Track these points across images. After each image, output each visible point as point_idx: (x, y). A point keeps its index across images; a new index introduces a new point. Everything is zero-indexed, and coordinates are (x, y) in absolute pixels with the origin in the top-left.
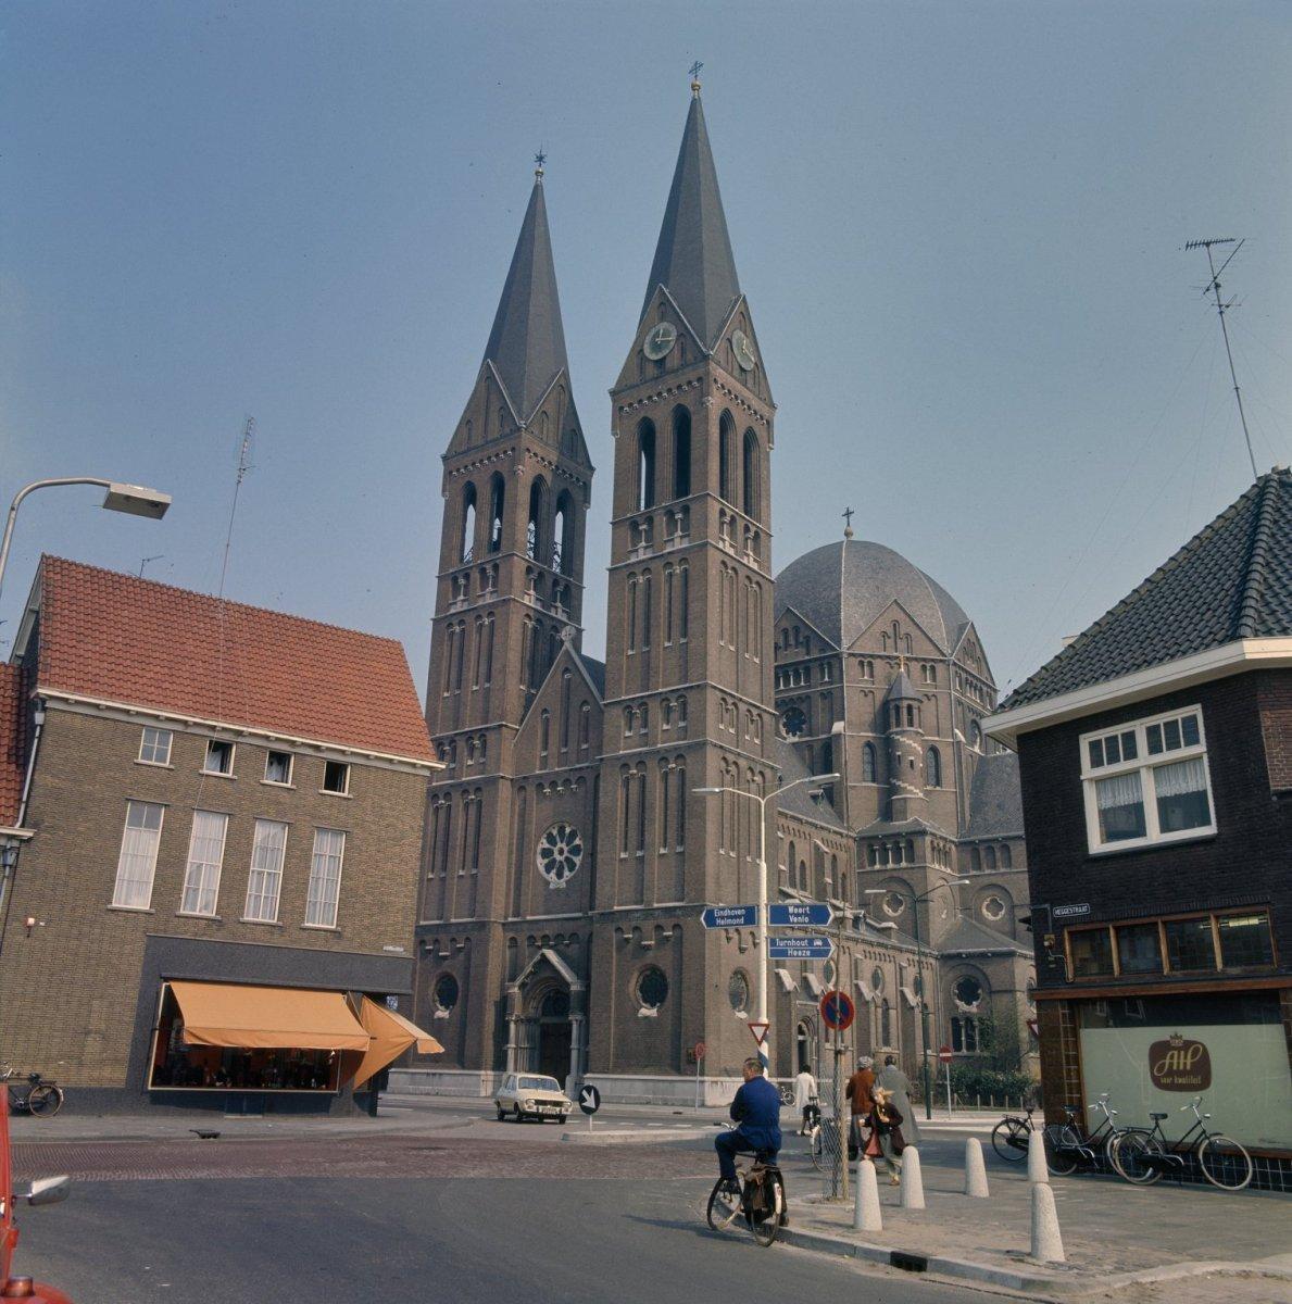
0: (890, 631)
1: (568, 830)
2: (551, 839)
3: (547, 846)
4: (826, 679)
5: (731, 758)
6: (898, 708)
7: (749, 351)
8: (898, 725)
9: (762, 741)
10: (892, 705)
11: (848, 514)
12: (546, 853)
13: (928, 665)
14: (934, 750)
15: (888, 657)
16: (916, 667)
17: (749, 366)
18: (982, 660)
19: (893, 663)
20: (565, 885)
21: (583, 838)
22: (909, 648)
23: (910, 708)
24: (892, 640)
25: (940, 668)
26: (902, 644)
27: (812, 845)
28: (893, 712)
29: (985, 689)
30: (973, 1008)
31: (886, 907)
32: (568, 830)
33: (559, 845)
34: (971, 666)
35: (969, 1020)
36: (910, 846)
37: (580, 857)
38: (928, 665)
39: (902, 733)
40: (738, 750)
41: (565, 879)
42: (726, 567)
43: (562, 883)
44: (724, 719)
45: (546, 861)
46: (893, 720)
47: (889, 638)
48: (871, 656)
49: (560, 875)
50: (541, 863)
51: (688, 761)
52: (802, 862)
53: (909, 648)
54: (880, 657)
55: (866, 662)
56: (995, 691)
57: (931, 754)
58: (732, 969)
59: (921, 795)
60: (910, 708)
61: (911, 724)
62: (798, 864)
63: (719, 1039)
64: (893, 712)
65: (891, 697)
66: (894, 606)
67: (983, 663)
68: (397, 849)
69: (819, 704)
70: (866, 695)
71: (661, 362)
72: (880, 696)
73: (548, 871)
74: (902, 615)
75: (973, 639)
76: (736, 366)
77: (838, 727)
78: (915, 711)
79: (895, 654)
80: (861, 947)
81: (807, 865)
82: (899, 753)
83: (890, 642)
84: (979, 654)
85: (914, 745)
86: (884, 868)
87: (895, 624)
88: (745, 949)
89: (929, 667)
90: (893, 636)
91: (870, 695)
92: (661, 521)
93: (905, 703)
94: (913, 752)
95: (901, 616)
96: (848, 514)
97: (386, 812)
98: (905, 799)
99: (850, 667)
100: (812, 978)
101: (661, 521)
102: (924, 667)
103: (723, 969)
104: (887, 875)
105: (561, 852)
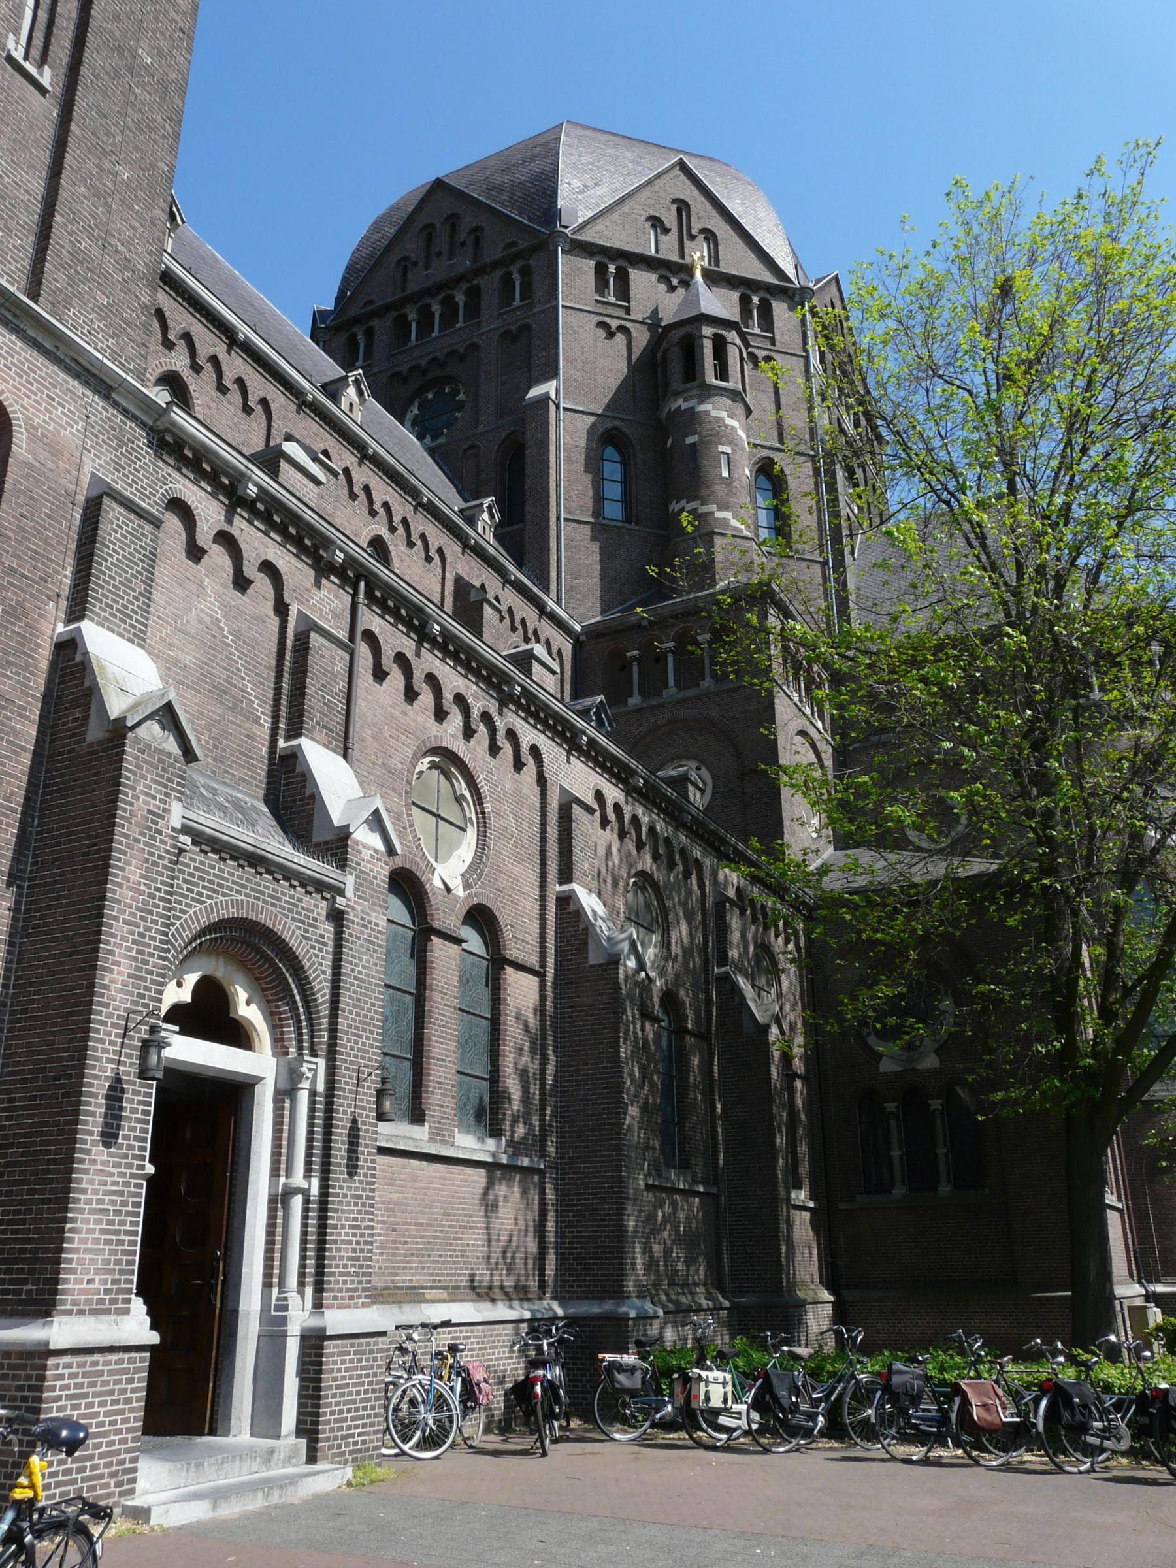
0: (670, 220)
4: (517, 303)
22: (715, 257)
24: (673, 236)
25: (779, 308)
39: (707, 392)
47: (667, 231)
53: (715, 257)
60: (720, 346)
61: (722, 371)
66: (677, 172)
70: (611, 335)
74: (696, 193)
82: (689, 440)
85: (729, 421)
87: (682, 206)
90: (675, 230)
91: (620, 338)
94: (732, 440)
95: (690, 193)
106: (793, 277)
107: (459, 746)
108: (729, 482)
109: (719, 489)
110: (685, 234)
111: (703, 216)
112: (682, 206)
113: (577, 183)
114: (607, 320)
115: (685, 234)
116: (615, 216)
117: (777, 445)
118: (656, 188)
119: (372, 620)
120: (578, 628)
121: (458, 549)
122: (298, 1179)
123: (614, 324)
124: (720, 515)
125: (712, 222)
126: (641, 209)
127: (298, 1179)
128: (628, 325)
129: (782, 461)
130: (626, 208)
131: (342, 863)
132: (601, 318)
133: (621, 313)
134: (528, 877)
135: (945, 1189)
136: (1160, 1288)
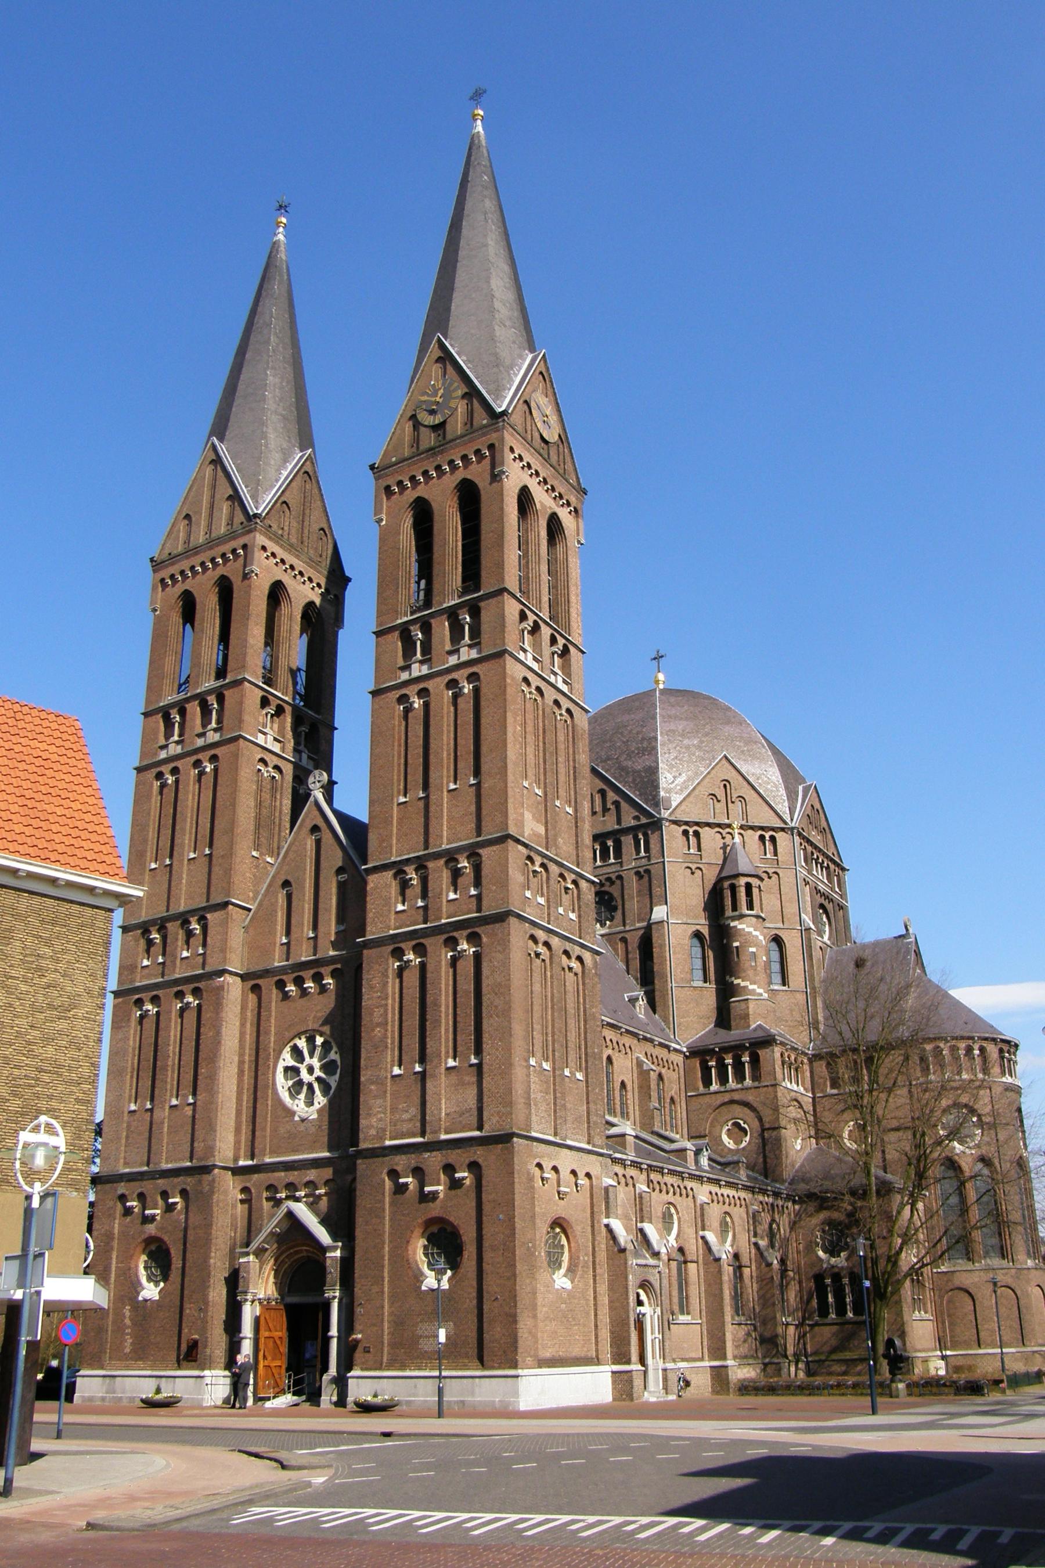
1: (319, 1040)
2: (297, 1053)
3: (291, 1063)
5: (541, 935)
6: (733, 888)
7: (553, 419)
8: (735, 908)
9: (579, 916)
10: (726, 884)
11: (658, 658)
12: (291, 1071)
13: (767, 835)
14: (777, 940)
15: (719, 825)
16: (753, 836)
17: (552, 436)
18: (826, 831)
19: (724, 832)
20: (315, 1116)
21: (342, 1051)
22: (745, 814)
23: (749, 887)
26: (736, 808)
27: (635, 1061)
28: (728, 893)
29: (832, 866)
30: (840, 1261)
31: (725, 1138)
32: (319, 1040)
33: (308, 1060)
34: (816, 838)
35: (837, 1277)
36: (755, 1060)
37: (337, 1077)
38: (767, 835)
40: (550, 926)
41: (317, 1106)
42: (528, 684)
43: (312, 1113)
44: (531, 885)
45: (290, 1083)
46: (728, 902)
47: (719, 801)
48: (697, 824)
49: (310, 1102)
50: (282, 1083)
51: (485, 939)
52: (623, 1084)
53: (745, 814)
54: (708, 825)
55: (692, 830)
56: (843, 869)
57: (774, 946)
58: (549, 1221)
59: (766, 995)
60: (749, 887)
61: (751, 907)
62: (617, 1085)
63: (535, 1317)
64: (728, 893)
65: (723, 875)
66: (724, 761)
67: (829, 836)
68: (63, 1025)
69: (632, 884)
70: (693, 873)
71: (439, 428)
72: (711, 876)
73: (293, 1096)
75: (817, 806)
76: (536, 435)
77: (659, 912)
78: (755, 891)
79: (727, 821)
80: (707, 1187)
81: (629, 1087)
82: (736, 944)
83: (720, 807)
84: (824, 824)
85: (755, 933)
86: (722, 1089)
87: (726, 784)
88: (566, 1194)
89: (768, 836)
91: (698, 873)
92: (442, 629)
93: (743, 881)
95: (732, 775)
96: (658, 658)
97: (44, 963)
98: (747, 1000)
99: (672, 835)
100: (650, 1229)
101: (442, 629)
102: (762, 838)
103: (538, 1221)
104: (727, 1098)
105: (311, 1070)
106: (788, 820)
107: (672, 1200)
108: (755, 968)
109: (750, 973)
110: (728, 801)
111: (740, 788)
112: (726, 784)
113: (670, 777)
114: (690, 865)
115: (728, 801)
116: (691, 799)
117: (780, 925)
118: (712, 775)
119: (653, 1176)
120: (685, 1050)
121: (636, 1041)
122: (657, 1335)
123: (693, 866)
124: (751, 987)
125: (743, 791)
126: (704, 791)
127: (657, 1335)
128: (701, 866)
129: (784, 935)
130: (696, 792)
131: (659, 1259)
132: (687, 865)
133: (697, 859)
134: (692, 1231)
135: (850, 1315)
136: (948, 1353)
